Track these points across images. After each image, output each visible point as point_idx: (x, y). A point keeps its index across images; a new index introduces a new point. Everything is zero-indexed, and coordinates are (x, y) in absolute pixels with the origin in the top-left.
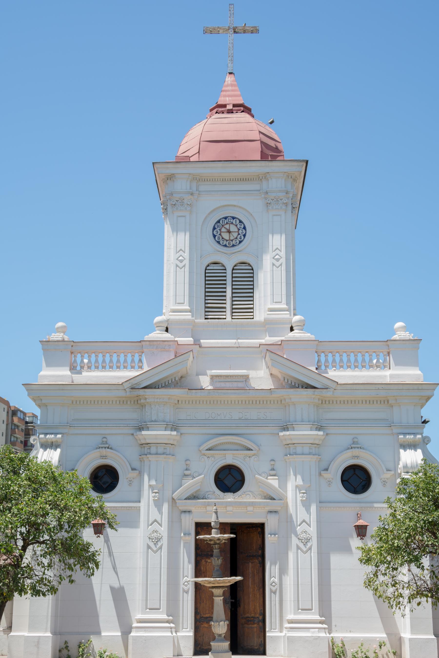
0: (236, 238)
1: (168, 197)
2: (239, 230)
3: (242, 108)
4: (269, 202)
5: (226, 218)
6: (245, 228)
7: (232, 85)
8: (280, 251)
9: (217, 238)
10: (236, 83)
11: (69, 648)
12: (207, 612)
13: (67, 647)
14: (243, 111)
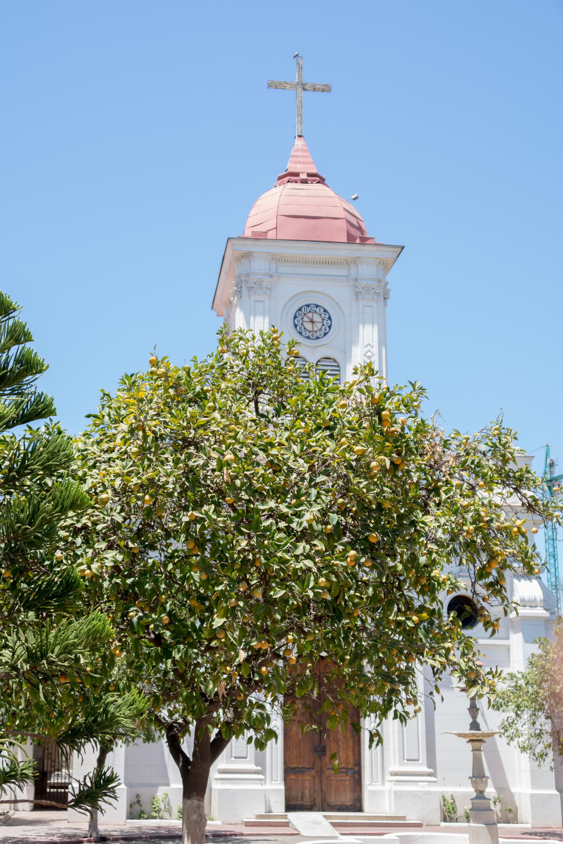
0: (321, 329)
1: (243, 278)
2: (323, 320)
3: (318, 179)
4: (359, 291)
5: (308, 306)
6: (330, 318)
7: (302, 150)
8: (372, 347)
9: (298, 328)
10: (306, 148)
11: (141, 803)
12: (294, 761)
13: (138, 802)
14: (318, 182)
